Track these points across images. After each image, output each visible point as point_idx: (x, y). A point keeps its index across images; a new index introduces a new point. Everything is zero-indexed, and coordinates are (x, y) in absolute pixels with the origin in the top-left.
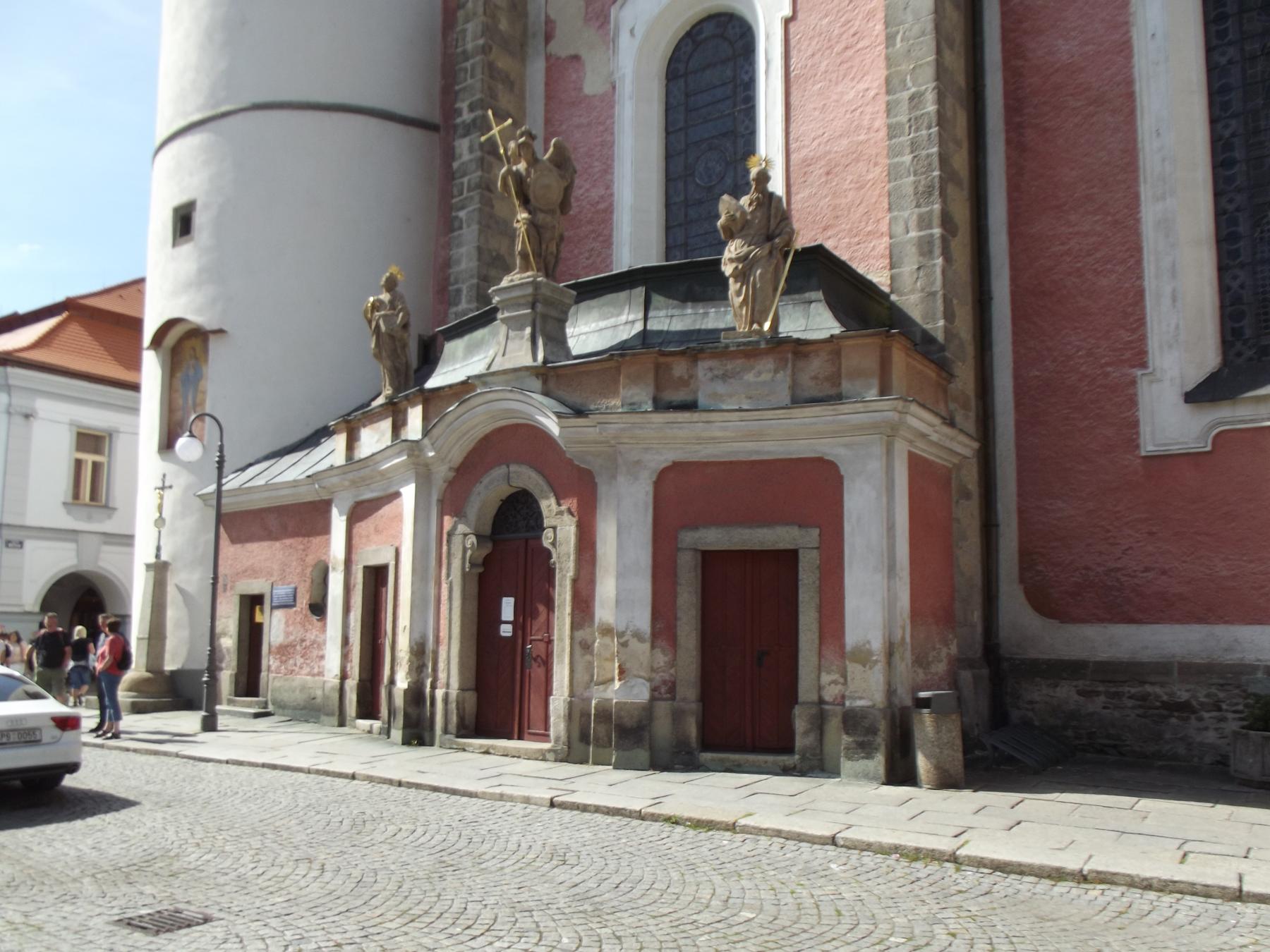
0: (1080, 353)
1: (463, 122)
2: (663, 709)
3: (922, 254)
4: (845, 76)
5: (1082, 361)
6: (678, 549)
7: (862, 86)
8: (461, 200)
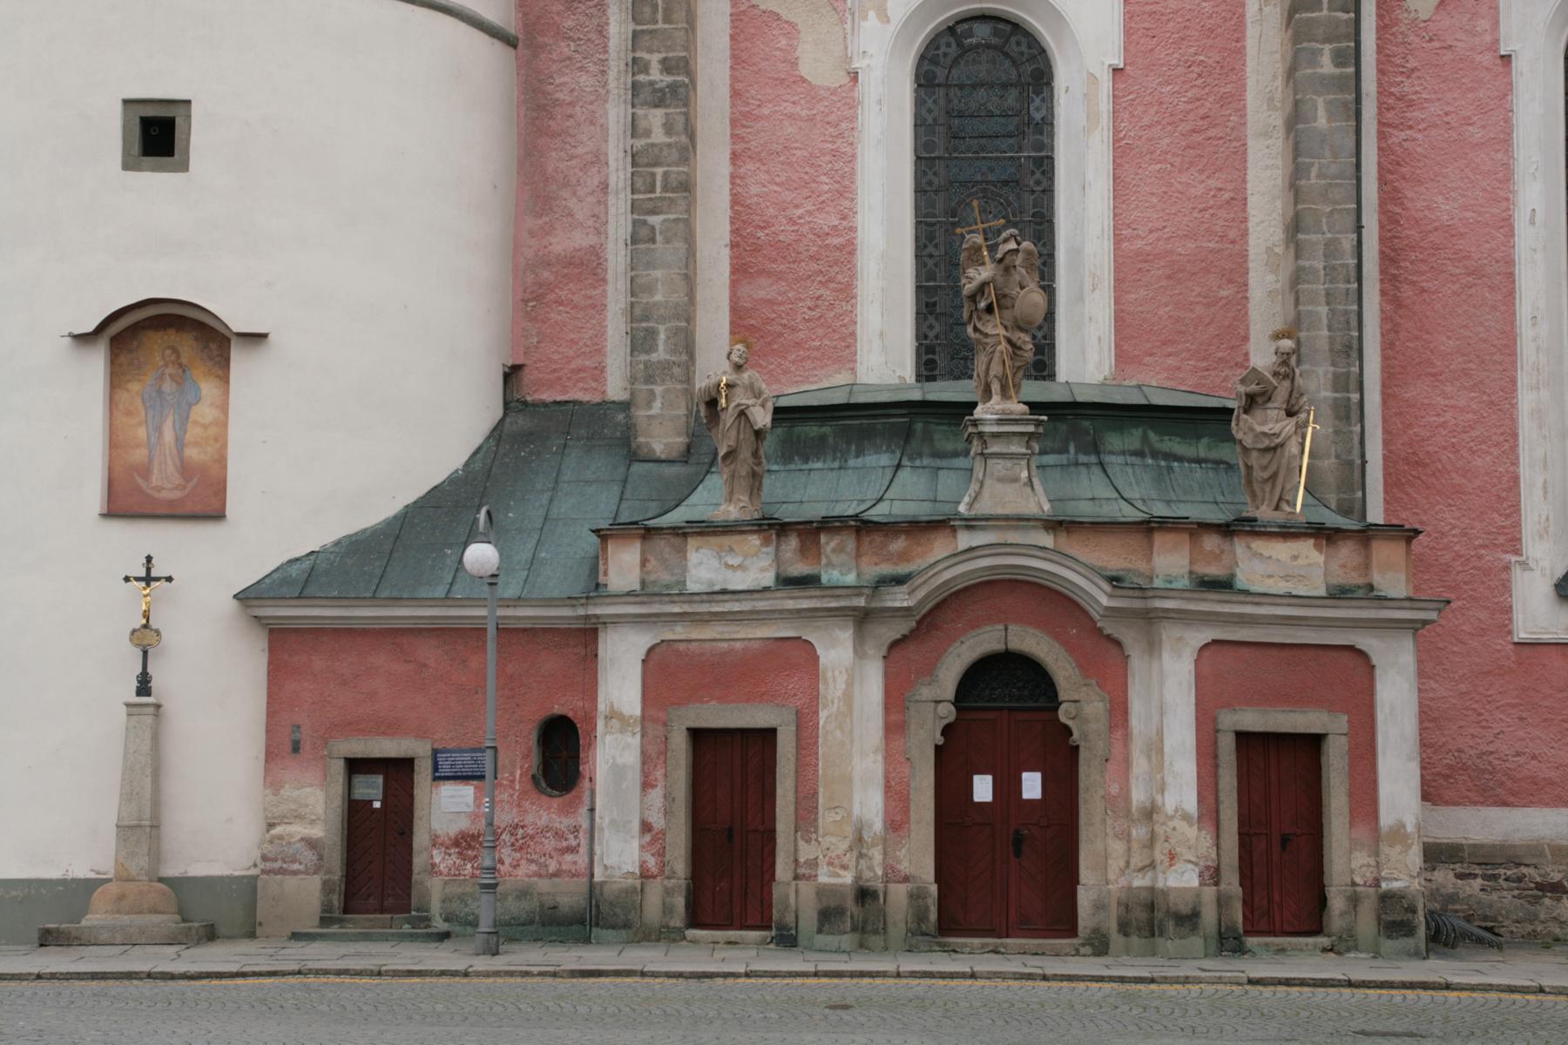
0: (1454, 532)
1: (652, 83)
2: (1209, 893)
3: (1338, 418)
4: (1191, 164)
5: (1456, 540)
6: (1217, 731)
7: (1212, 183)
8: (651, 199)
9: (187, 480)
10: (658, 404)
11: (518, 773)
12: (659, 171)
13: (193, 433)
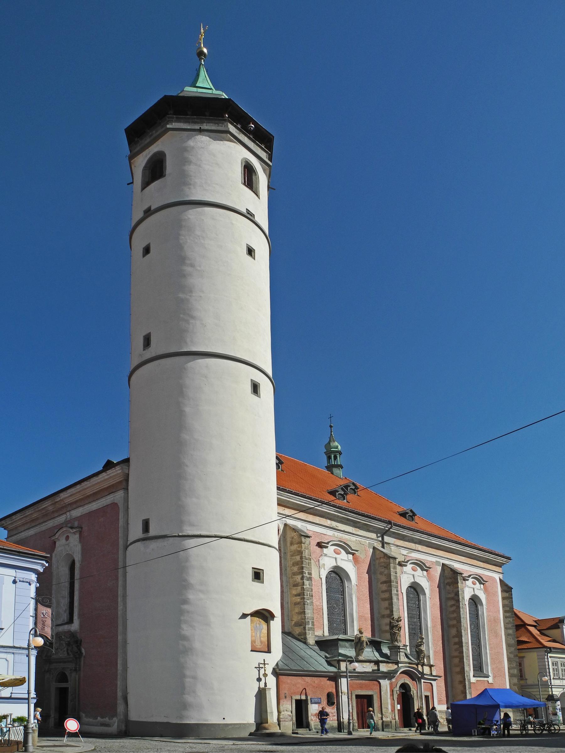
1: (306, 576)
9: (262, 644)
10: (310, 635)
11: (325, 702)
12: (308, 592)
13: (262, 635)
